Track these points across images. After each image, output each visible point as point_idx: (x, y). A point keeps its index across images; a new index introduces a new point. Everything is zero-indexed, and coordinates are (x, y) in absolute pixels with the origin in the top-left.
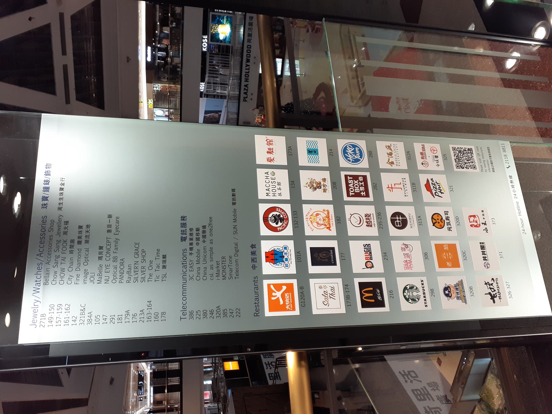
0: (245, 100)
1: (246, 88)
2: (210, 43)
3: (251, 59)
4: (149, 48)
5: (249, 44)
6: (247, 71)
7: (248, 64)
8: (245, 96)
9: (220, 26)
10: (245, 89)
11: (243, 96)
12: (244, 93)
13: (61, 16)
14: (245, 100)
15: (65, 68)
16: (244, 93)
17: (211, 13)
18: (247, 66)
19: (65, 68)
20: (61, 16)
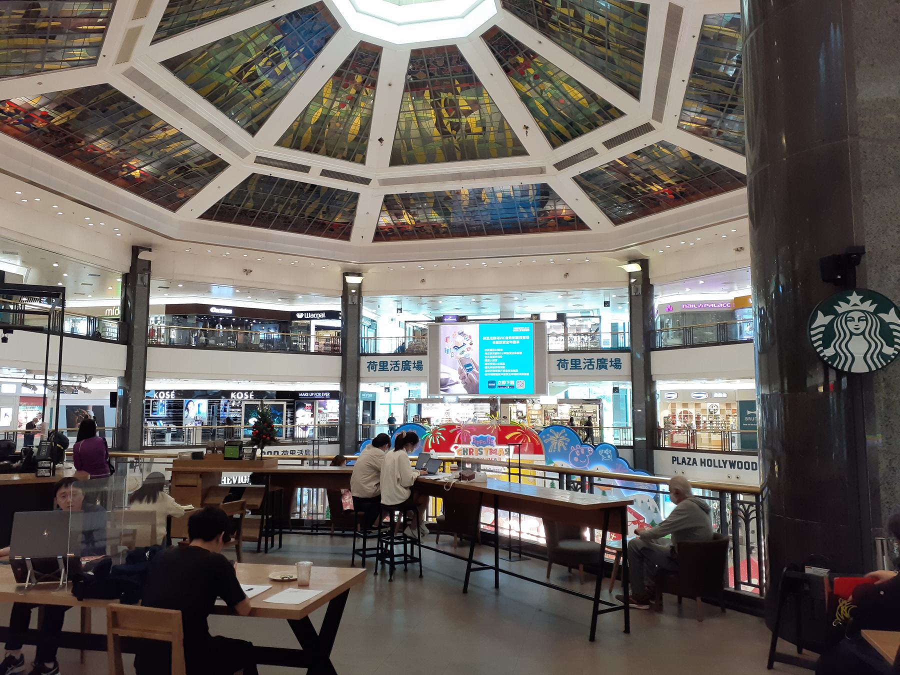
13: (646, 128)
15: (591, 153)
19: (591, 153)
20: (646, 128)
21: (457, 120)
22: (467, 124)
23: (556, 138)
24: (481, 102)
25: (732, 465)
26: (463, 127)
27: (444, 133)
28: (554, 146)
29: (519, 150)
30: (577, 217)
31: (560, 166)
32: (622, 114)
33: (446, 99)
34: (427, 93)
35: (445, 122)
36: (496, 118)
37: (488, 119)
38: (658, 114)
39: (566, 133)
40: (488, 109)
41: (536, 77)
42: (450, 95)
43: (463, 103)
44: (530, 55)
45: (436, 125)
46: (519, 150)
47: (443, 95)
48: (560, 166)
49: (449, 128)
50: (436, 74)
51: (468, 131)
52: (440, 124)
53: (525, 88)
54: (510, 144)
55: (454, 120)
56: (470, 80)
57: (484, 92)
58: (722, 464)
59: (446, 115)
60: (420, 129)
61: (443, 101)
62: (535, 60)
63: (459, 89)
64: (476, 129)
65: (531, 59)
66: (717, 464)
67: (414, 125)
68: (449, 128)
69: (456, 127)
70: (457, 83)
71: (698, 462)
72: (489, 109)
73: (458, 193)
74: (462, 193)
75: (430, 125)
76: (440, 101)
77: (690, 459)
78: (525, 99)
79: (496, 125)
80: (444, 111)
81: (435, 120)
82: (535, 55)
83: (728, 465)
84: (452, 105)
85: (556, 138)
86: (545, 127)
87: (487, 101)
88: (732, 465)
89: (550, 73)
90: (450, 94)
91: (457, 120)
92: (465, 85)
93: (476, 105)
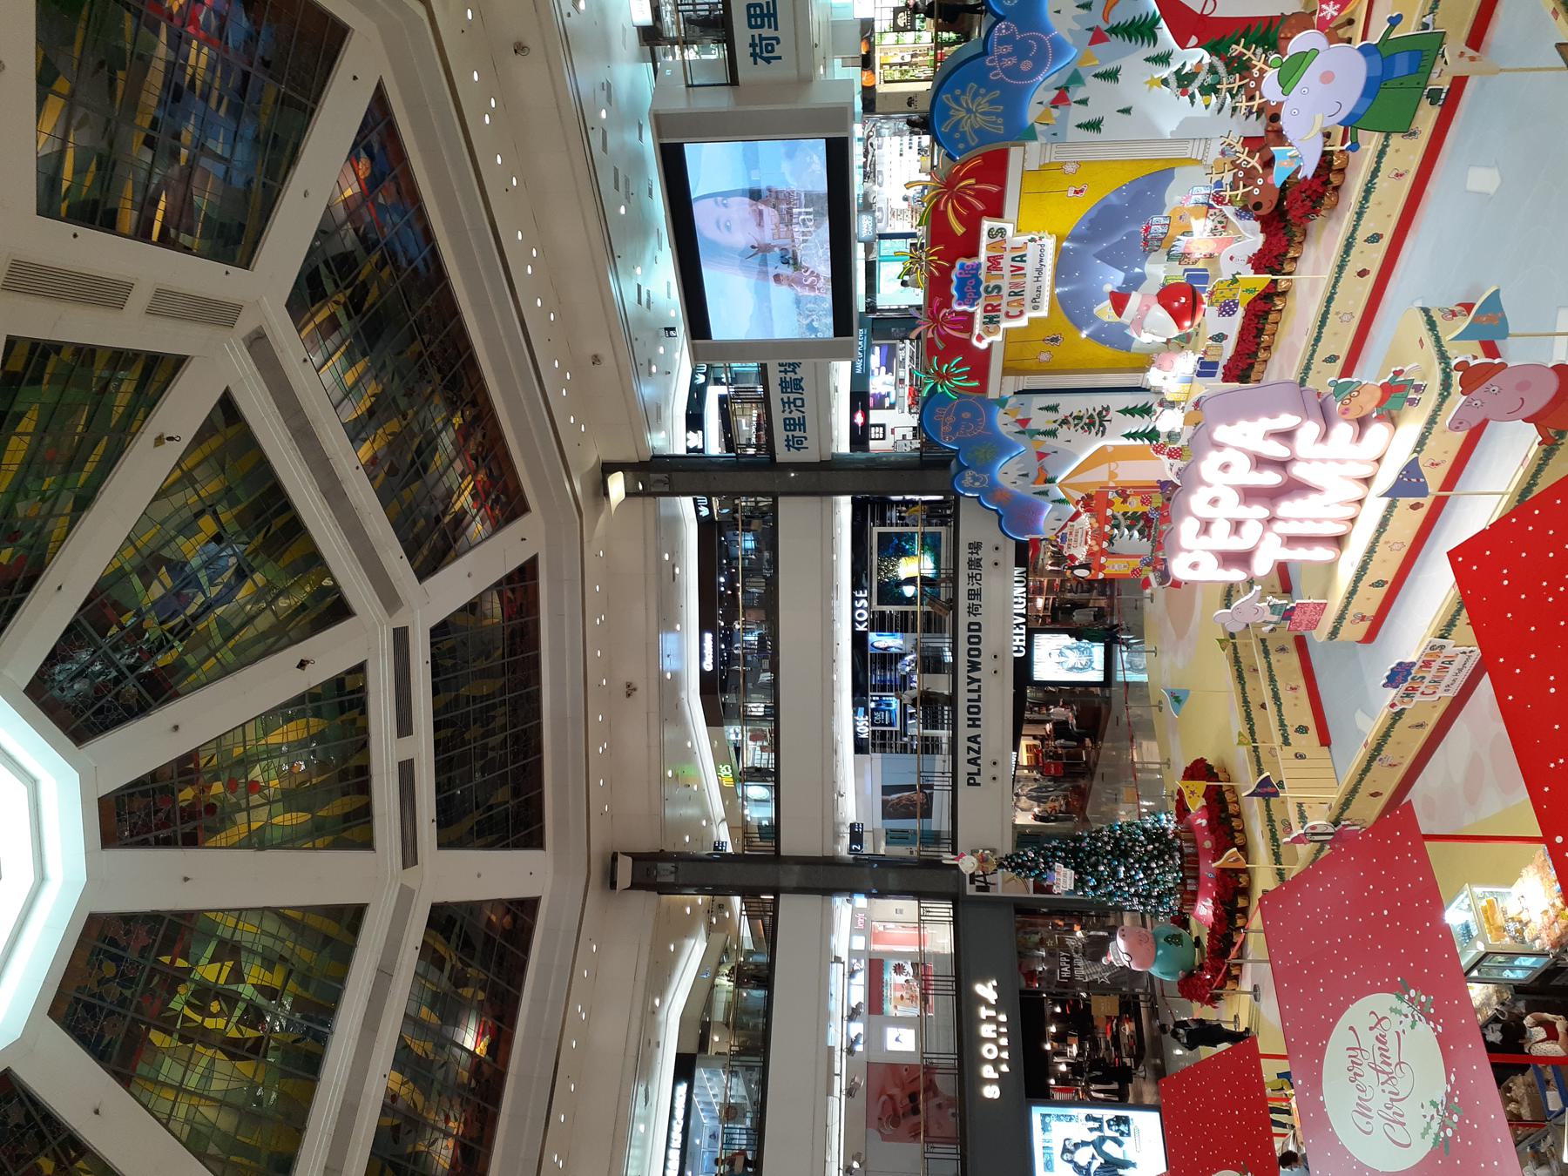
0: (972, 781)
1: (975, 746)
2: (877, 608)
3: (985, 660)
4: (708, 637)
5: (973, 619)
6: (974, 696)
7: (974, 675)
8: (974, 769)
9: (903, 560)
10: (969, 748)
11: (964, 769)
12: (969, 761)
13: (401, 638)
14: (972, 781)
15: (406, 770)
16: (969, 761)
17: (876, 530)
18: (973, 680)
19: (406, 770)
20: (401, 638)
21: (242, 1005)
22: (260, 989)
23: (353, 830)
24: (227, 935)
25: (974, 666)
26: (261, 1000)
27: (255, 1050)
28: (368, 845)
29: (351, 917)
30: (511, 902)
31: (410, 856)
32: (361, 668)
33: (188, 1003)
34: (156, 1037)
35: (233, 1033)
36: (271, 925)
37: (269, 942)
38: (390, 599)
39: (356, 801)
40: (247, 933)
41: (232, 785)
42: (184, 992)
43: (210, 972)
44: (186, 767)
45: (232, 1057)
46: (351, 917)
47: (177, 1004)
48: (410, 856)
49: (250, 1033)
50: (128, 993)
51: (271, 993)
52: (235, 1050)
53: (240, 830)
54: (331, 928)
55: (238, 1013)
56: (174, 929)
57: (212, 915)
58: (974, 686)
59: (220, 1023)
60: (221, 1103)
61: (188, 1012)
62: (202, 762)
63: (181, 963)
64: (275, 979)
65: (197, 769)
66: (974, 696)
67: (210, 1113)
68: (250, 1033)
69: (254, 1016)
70: (166, 959)
71: (973, 732)
72: (248, 927)
73: (392, 1097)
74: (396, 1088)
75: (225, 1075)
76: (186, 1019)
77: (969, 748)
78: (258, 841)
79: (284, 932)
80: (210, 1023)
81: (220, 1055)
82: (192, 756)
83: (974, 675)
84: (204, 995)
85: (353, 830)
86: (328, 839)
87: (231, 922)
88: (974, 666)
89: (238, 751)
90: (181, 989)
91: (242, 1005)
92: (178, 948)
93: (229, 950)
